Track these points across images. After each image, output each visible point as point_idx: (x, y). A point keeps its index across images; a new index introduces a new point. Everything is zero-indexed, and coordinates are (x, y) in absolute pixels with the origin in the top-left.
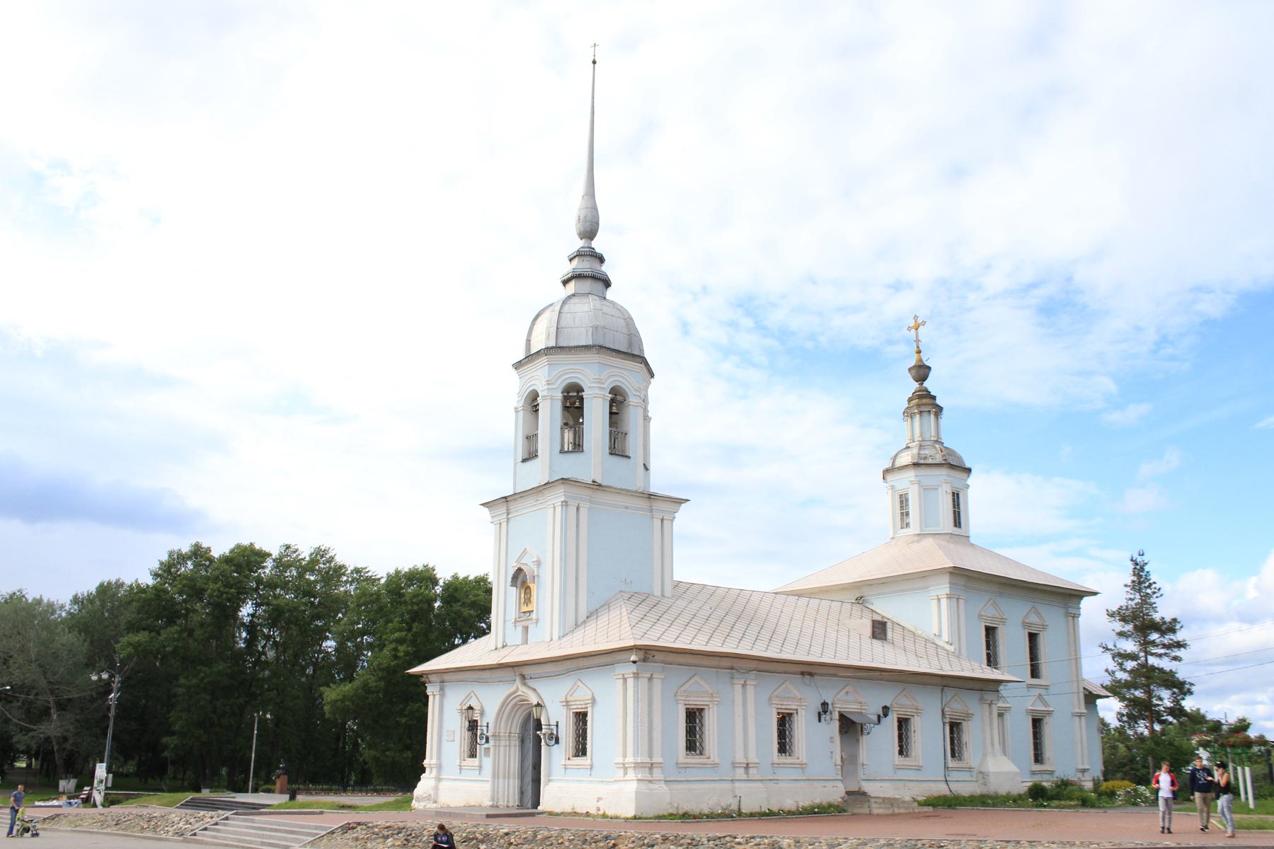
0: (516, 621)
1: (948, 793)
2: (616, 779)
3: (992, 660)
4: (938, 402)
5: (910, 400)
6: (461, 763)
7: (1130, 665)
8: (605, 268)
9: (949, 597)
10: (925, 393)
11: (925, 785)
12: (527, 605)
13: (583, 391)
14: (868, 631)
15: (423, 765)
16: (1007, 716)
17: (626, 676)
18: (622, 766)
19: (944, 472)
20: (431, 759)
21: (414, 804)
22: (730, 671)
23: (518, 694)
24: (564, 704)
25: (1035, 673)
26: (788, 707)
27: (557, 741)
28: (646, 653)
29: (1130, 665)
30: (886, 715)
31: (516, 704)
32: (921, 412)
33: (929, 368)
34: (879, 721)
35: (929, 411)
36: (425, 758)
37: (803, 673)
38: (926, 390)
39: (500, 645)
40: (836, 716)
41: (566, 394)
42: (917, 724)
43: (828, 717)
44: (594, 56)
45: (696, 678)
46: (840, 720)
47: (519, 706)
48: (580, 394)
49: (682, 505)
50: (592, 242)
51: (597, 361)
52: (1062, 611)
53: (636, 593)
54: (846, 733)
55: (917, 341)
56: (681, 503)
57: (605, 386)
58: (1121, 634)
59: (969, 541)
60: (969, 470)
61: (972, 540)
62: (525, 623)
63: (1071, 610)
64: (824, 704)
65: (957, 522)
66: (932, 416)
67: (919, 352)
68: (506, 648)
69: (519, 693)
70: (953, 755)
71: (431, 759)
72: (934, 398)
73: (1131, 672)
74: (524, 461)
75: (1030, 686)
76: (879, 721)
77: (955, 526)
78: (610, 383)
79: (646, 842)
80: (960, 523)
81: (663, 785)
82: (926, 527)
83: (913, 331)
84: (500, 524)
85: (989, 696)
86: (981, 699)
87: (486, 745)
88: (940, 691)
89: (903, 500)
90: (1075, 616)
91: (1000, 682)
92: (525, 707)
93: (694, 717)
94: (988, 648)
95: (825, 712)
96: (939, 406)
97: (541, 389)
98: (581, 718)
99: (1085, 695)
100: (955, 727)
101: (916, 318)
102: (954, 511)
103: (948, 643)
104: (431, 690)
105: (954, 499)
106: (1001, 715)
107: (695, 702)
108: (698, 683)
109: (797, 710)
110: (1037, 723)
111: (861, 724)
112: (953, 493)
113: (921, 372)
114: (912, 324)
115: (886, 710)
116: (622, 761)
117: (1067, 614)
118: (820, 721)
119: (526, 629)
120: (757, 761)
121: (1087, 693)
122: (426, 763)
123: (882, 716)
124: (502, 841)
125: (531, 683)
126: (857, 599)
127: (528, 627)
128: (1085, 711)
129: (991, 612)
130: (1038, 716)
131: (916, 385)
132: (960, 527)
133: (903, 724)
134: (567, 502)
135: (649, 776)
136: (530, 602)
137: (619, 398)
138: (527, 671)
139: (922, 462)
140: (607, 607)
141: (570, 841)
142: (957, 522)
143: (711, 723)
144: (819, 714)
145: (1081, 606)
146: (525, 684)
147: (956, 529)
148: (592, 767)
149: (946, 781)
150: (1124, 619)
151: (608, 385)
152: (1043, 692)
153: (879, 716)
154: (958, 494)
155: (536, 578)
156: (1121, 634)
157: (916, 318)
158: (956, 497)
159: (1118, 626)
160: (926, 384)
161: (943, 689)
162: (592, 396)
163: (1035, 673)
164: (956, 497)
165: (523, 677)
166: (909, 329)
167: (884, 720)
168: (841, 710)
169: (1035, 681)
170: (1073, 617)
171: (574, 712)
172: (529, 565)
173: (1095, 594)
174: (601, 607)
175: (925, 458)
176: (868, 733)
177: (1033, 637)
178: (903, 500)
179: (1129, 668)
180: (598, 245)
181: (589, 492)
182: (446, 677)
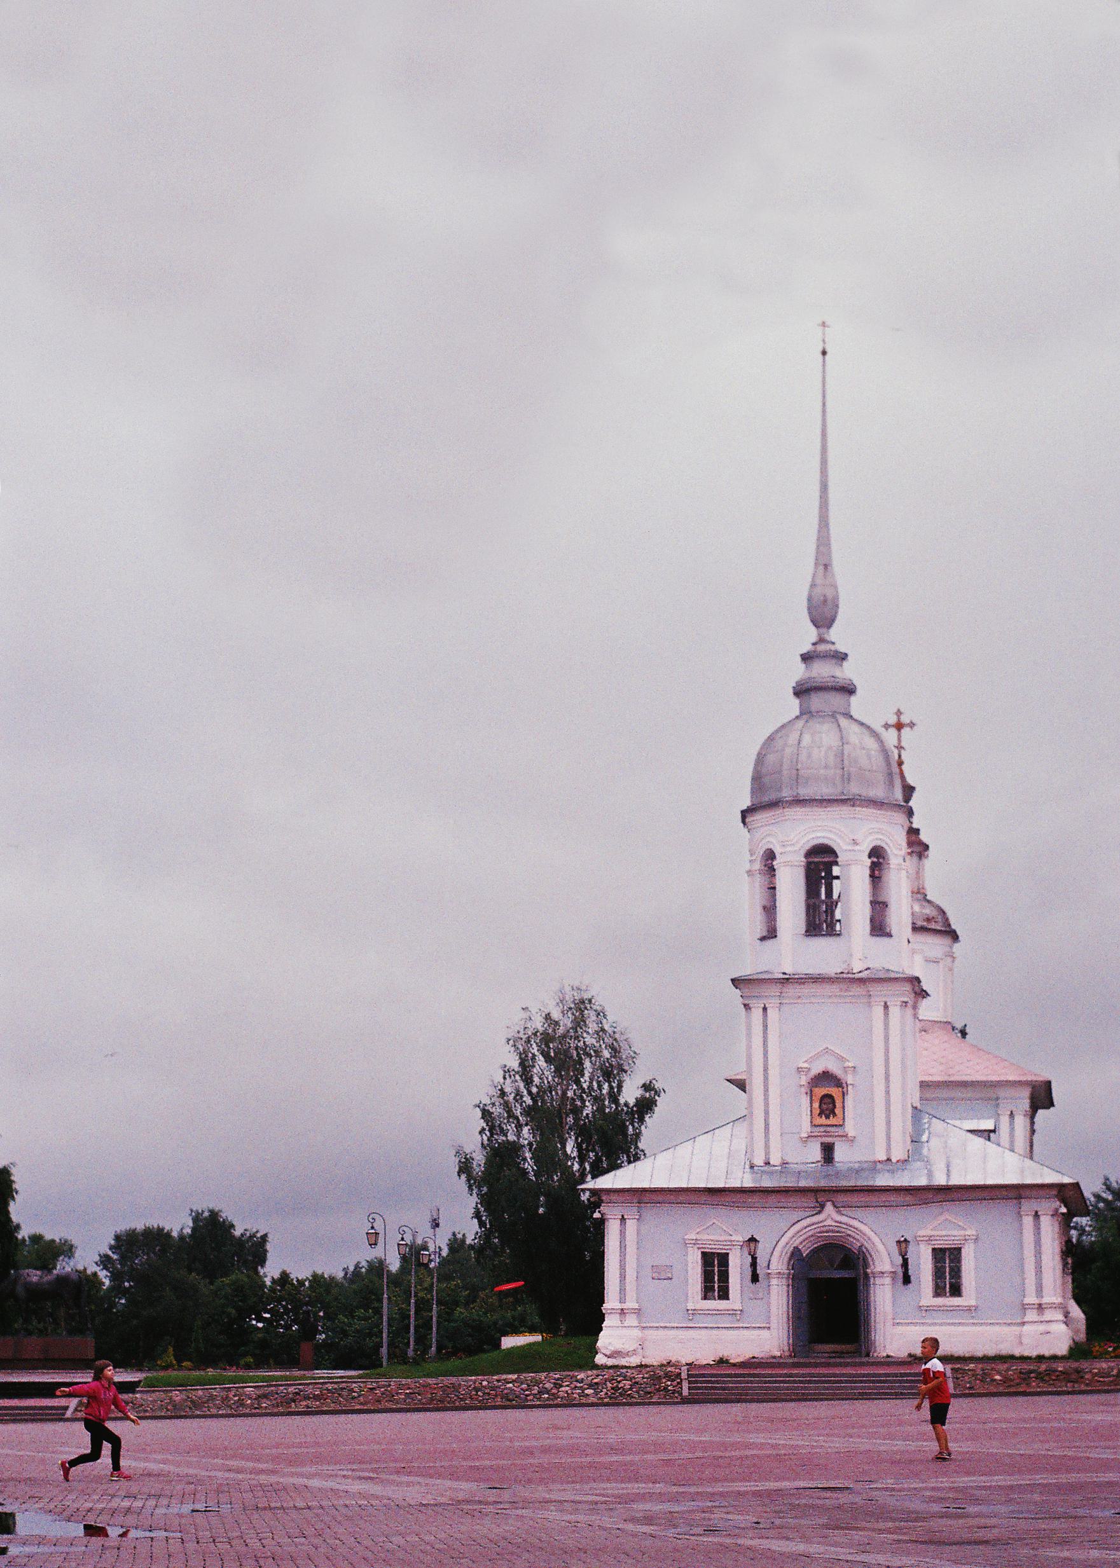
12: (827, 1117)
20: (622, 1300)
21: (600, 1359)
23: (825, 1223)
27: (907, 1280)
39: (775, 1160)
48: (881, 860)
69: (829, 1222)
71: (622, 1300)
101: (899, 713)
114: (893, 720)
116: (1037, 1301)
122: (606, 1306)
136: (835, 1115)
138: (841, 1198)
146: (839, 1213)
157: (899, 713)
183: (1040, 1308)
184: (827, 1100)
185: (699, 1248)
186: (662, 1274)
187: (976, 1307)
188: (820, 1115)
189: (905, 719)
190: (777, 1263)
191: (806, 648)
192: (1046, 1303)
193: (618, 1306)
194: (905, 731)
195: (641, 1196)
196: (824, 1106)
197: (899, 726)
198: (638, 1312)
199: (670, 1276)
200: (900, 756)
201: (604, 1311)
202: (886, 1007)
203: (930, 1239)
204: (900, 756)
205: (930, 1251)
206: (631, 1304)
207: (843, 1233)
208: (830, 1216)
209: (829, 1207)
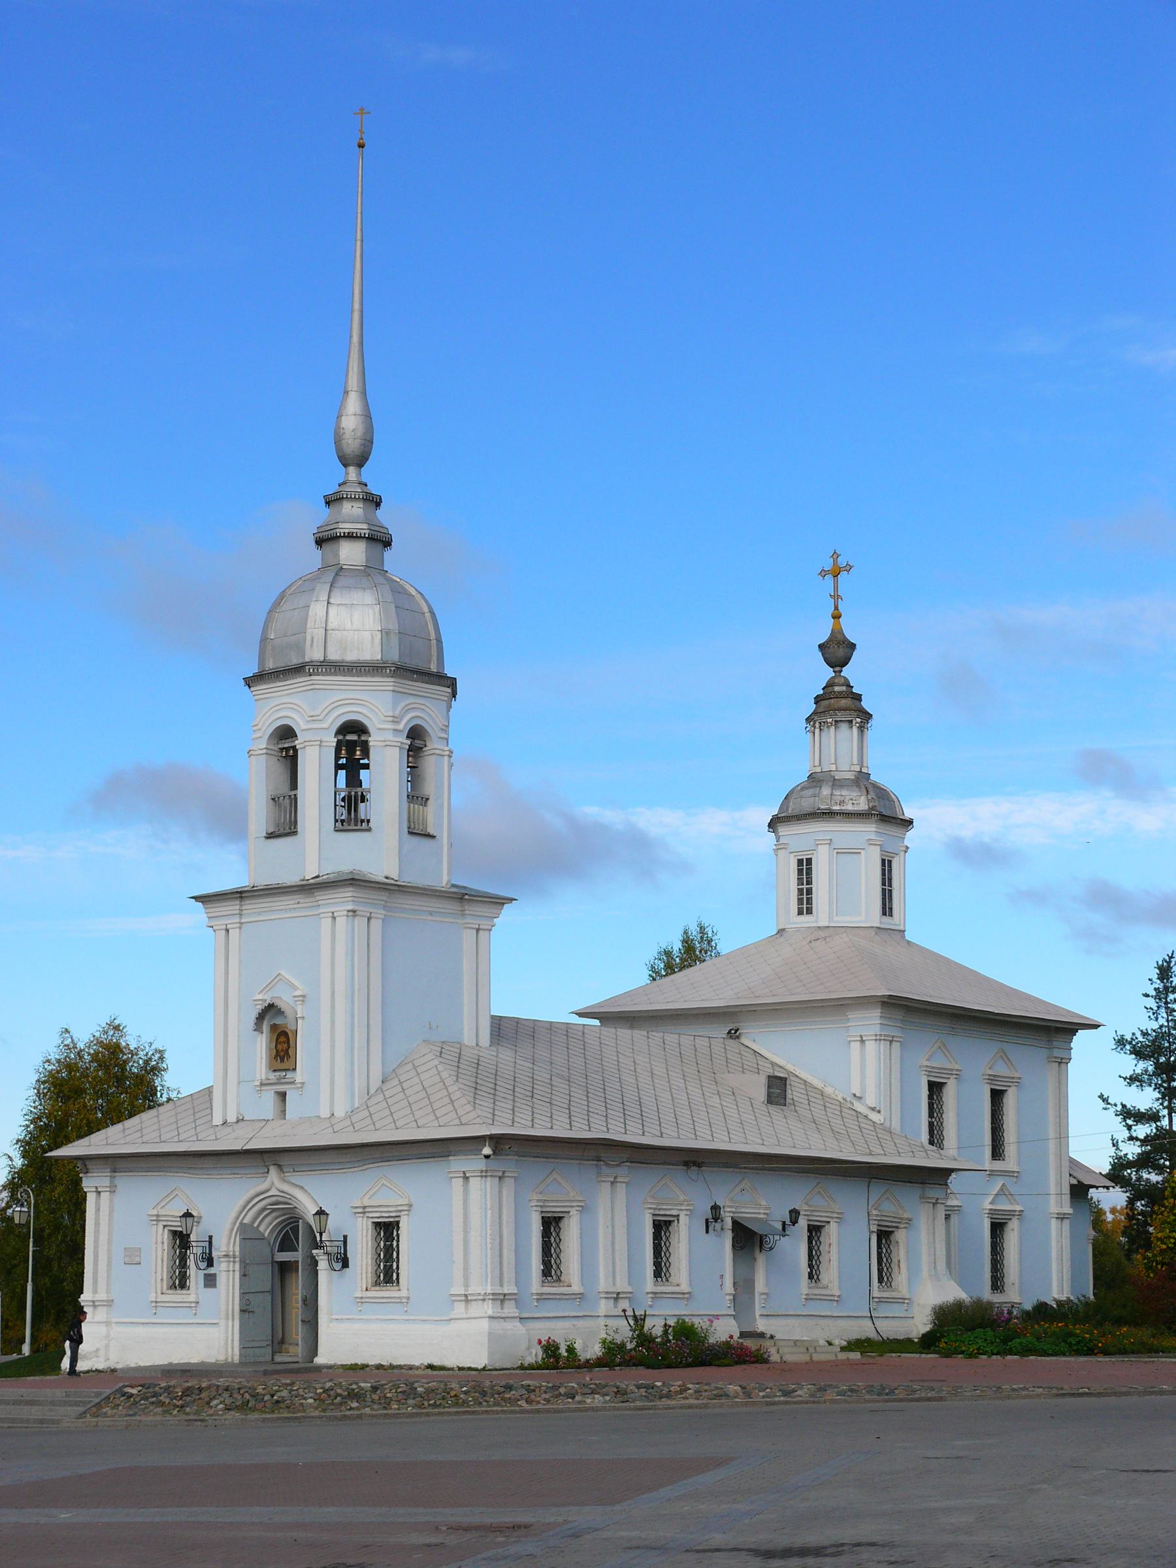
0: (262, 1084)
1: (872, 1335)
2: (452, 1317)
3: (935, 1135)
4: (865, 704)
5: (818, 700)
6: (156, 1297)
7: (1142, 1131)
8: (383, 515)
9: (878, 1039)
10: (844, 688)
11: (841, 1322)
12: (282, 1060)
13: (370, 736)
14: (761, 1093)
15: (78, 1301)
16: (954, 1219)
17: (467, 1175)
18: (463, 1298)
19: (868, 830)
20: (95, 1291)
22: (595, 1162)
24: (360, 1210)
25: (997, 1152)
26: (668, 1213)
27: (345, 1263)
28: (497, 1142)
29: (1142, 1131)
30: (794, 1222)
31: (264, 1209)
32: (836, 721)
33: (853, 646)
34: (784, 1229)
35: (851, 722)
36: (82, 1293)
37: (686, 1164)
39: (232, 1118)
40: (728, 1223)
41: (341, 737)
42: (832, 1234)
43: (718, 1226)
44: (361, 132)
45: (555, 1175)
46: (733, 1230)
47: (269, 1211)
48: (363, 738)
49: (505, 905)
51: (391, 688)
52: (1044, 1053)
53: (444, 1042)
54: (742, 1248)
55: (836, 597)
56: (504, 904)
57: (401, 727)
58: (1133, 1079)
59: (903, 937)
60: (910, 822)
61: (908, 936)
62: (281, 1088)
63: (1057, 1053)
64: (715, 1208)
65: (887, 909)
66: (855, 729)
67: (837, 616)
68: (241, 1124)
70: (880, 1280)
71: (95, 1291)
72: (858, 697)
73: (1145, 1141)
74: (271, 836)
75: (993, 1173)
76: (784, 1229)
77: (884, 914)
78: (407, 723)
79: (562, 1390)
80: (891, 909)
81: (518, 1324)
83: (829, 579)
84: (227, 930)
85: (934, 1192)
86: (922, 1197)
87: (211, 1271)
88: (866, 1185)
89: (805, 868)
90: (1063, 1062)
91: (949, 1172)
92: (274, 1214)
93: (551, 1225)
94: (931, 1115)
95: (716, 1219)
96: (869, 714)
97: (304, 727)
98: (387, 1230)
99: (1072, 1186)
100: (884, 1236)
101: (835, 555)
102: (884, 890)
103: (873, 1109)
104: (88, 1184)
105: (883, 871)
106: (947, 1217)
107: (554, 1208)
108: (557, 1181)
109: (678, 1215)
110: (998, 1228)
111: (761, 1236)
112: (883, 861)
115: (795, 1215)
117: (1052, 1059)
118: (707, 1232)
119: (283, 1096)
120: (630, 1290)
121: (1075, 1182)
122: (84, 1298)
123: (788, 1222)
124: (376, 1397)
125: (296, 1178)
126: (729, 1032)
127: (286, 1094)
128: (1070, 1211)
129: (939, 1062)
130: (1000, 1218)
131: (829, 673)
132: (891, 915)
133: (814, 1231)
134: (354, 911)
135: (500, 1311)
136: (289, 1057)
137: (418, 743)
138: (284, 1160)
139: (836, 808)
140: (410, 1066)
141: (466, 1393)
142: (887, 909)
143: (571, 1234)
144: (707, 1221)
145: (1072, 1045)
146: (284, 1180)
147: (886, 919)
148: (408, 1298)
149: (871, 1317)
150: (1139, 1053)
151: (404, 725)
152: (1009, 1182)
153: (784, 1223)
154: (890, 862)
155: (300, 1021)
156: (1133, 1079)
157: (835, 555)
158: (886, 866)
159: (1130, 1064)
160: (846, 672)
161: (869, 1186)
162: (384, 744)
163: (997, 1152)
164: (886, 866)
165: (280, 1167)
166: (823, 574)
167: (790, 1230)
168: (736, 1215)
169: (998, 1165)
170: (1060, 1063)
171: (373, 1222)
172: (284, 998)
173: (1096, 1026)
174: (400, 1066)
175: (842, 803)
176: (771, 1249)
177: (997, 1096)
178: (805, 868)
179: (1142, 1137)
180: (374, 476)
181: (383, 896)
182: (121, 1164)
183: (467, 1299)
184: (282, 1039)
185: (165, 1226)
186: (133, 1258)
187: (408, 1298)
188: (276, 1057)
189: (842, 562)
190: (226, 1244)
191: (332, 489)
192: (472, 1295)
195: (117, 1163)
196: (280, 1047)
198: (109, 1303)
199: (137, 1259)
200: (836, 608)
201: (82, 1304)
202: (334, 918)
203: (364, 1210)
204: (836, 608)
205: (370, 1226)
206: (102, 1296)
207: (290, 1204)
208: (274, 1183)
209: (273, 1171)
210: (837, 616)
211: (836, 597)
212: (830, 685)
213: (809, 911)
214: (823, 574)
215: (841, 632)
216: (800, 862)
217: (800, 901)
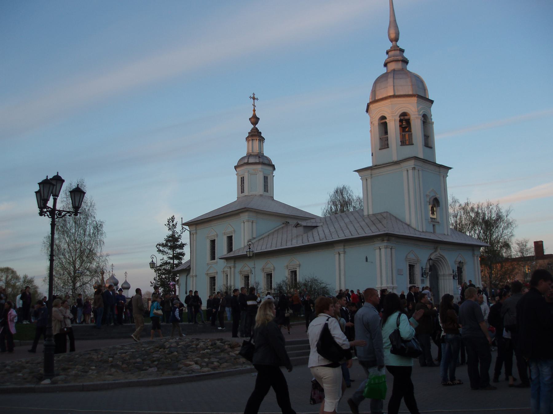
38: (257, 129)
50: (397, 43)
55: (254, 106)
67: (254, 111)
82: (251, 192)
101: (254, 94)
113: (255, 120)
131: (252, 126)
136: (434, 215)
160: (257, 126)
193: (392, 286)
194: (256, 101)
197: (254, 99)
200: (254, 108)
204: (254, 108)
210: (254, 111)
211: (254, 106)
212: (252, 129)
213: (267, 192)
214: (250, 97)
215: (255, 114)
216: (265, 177)
217: (265, 188)
